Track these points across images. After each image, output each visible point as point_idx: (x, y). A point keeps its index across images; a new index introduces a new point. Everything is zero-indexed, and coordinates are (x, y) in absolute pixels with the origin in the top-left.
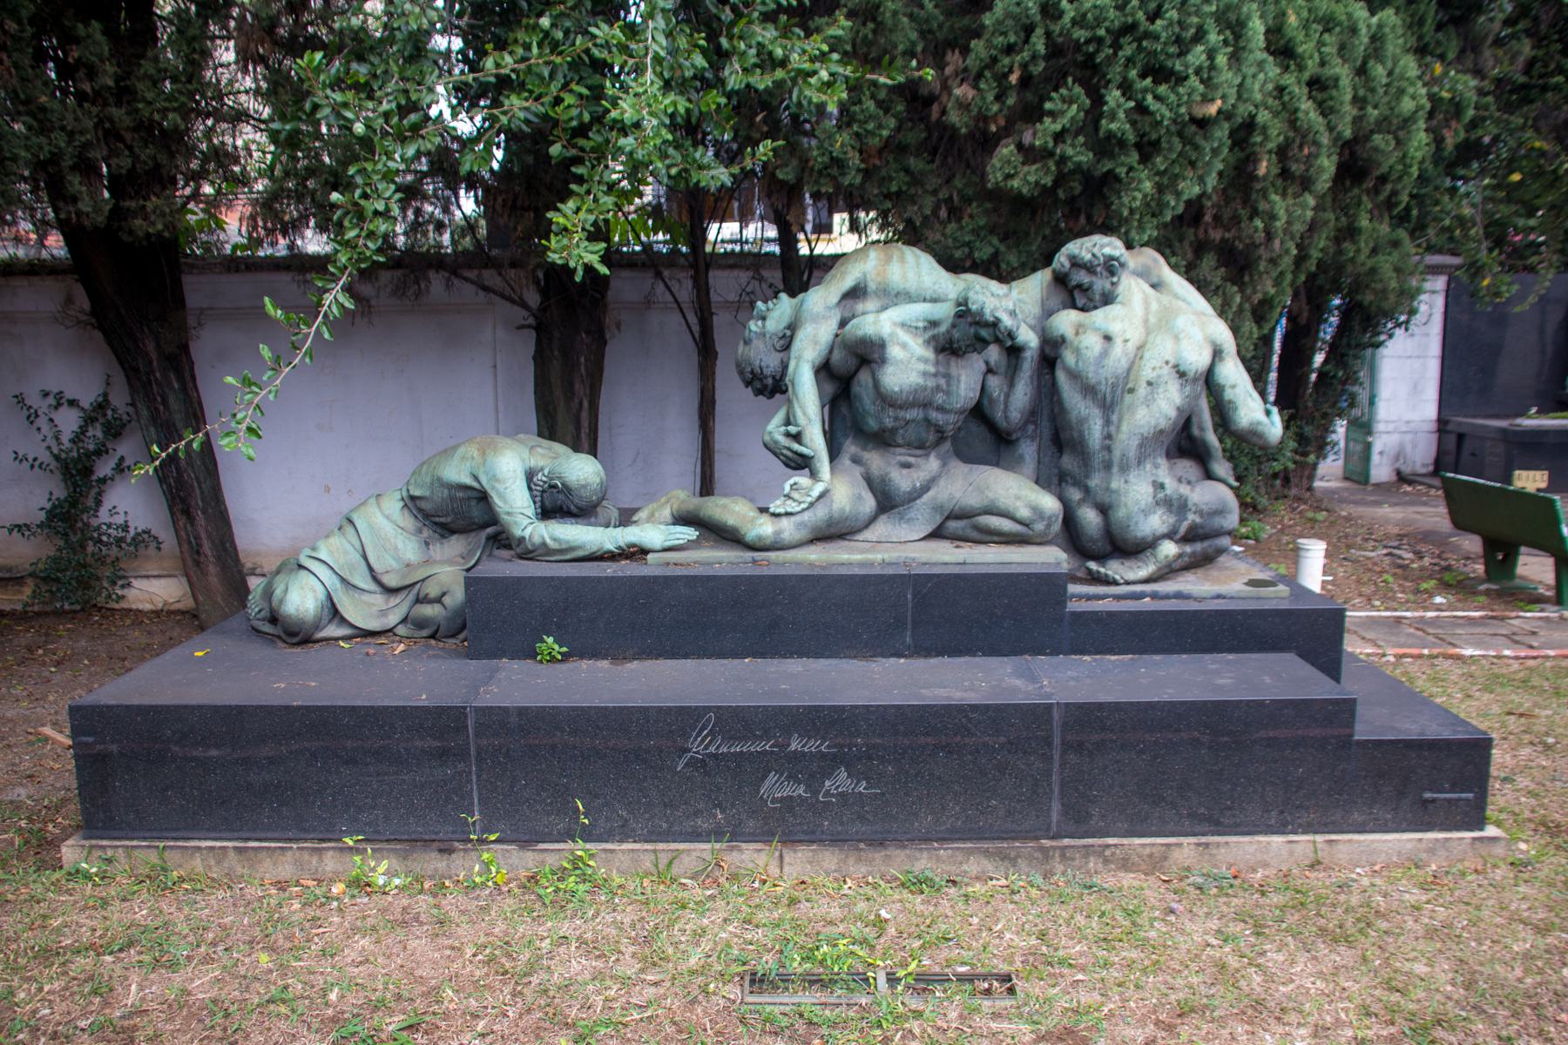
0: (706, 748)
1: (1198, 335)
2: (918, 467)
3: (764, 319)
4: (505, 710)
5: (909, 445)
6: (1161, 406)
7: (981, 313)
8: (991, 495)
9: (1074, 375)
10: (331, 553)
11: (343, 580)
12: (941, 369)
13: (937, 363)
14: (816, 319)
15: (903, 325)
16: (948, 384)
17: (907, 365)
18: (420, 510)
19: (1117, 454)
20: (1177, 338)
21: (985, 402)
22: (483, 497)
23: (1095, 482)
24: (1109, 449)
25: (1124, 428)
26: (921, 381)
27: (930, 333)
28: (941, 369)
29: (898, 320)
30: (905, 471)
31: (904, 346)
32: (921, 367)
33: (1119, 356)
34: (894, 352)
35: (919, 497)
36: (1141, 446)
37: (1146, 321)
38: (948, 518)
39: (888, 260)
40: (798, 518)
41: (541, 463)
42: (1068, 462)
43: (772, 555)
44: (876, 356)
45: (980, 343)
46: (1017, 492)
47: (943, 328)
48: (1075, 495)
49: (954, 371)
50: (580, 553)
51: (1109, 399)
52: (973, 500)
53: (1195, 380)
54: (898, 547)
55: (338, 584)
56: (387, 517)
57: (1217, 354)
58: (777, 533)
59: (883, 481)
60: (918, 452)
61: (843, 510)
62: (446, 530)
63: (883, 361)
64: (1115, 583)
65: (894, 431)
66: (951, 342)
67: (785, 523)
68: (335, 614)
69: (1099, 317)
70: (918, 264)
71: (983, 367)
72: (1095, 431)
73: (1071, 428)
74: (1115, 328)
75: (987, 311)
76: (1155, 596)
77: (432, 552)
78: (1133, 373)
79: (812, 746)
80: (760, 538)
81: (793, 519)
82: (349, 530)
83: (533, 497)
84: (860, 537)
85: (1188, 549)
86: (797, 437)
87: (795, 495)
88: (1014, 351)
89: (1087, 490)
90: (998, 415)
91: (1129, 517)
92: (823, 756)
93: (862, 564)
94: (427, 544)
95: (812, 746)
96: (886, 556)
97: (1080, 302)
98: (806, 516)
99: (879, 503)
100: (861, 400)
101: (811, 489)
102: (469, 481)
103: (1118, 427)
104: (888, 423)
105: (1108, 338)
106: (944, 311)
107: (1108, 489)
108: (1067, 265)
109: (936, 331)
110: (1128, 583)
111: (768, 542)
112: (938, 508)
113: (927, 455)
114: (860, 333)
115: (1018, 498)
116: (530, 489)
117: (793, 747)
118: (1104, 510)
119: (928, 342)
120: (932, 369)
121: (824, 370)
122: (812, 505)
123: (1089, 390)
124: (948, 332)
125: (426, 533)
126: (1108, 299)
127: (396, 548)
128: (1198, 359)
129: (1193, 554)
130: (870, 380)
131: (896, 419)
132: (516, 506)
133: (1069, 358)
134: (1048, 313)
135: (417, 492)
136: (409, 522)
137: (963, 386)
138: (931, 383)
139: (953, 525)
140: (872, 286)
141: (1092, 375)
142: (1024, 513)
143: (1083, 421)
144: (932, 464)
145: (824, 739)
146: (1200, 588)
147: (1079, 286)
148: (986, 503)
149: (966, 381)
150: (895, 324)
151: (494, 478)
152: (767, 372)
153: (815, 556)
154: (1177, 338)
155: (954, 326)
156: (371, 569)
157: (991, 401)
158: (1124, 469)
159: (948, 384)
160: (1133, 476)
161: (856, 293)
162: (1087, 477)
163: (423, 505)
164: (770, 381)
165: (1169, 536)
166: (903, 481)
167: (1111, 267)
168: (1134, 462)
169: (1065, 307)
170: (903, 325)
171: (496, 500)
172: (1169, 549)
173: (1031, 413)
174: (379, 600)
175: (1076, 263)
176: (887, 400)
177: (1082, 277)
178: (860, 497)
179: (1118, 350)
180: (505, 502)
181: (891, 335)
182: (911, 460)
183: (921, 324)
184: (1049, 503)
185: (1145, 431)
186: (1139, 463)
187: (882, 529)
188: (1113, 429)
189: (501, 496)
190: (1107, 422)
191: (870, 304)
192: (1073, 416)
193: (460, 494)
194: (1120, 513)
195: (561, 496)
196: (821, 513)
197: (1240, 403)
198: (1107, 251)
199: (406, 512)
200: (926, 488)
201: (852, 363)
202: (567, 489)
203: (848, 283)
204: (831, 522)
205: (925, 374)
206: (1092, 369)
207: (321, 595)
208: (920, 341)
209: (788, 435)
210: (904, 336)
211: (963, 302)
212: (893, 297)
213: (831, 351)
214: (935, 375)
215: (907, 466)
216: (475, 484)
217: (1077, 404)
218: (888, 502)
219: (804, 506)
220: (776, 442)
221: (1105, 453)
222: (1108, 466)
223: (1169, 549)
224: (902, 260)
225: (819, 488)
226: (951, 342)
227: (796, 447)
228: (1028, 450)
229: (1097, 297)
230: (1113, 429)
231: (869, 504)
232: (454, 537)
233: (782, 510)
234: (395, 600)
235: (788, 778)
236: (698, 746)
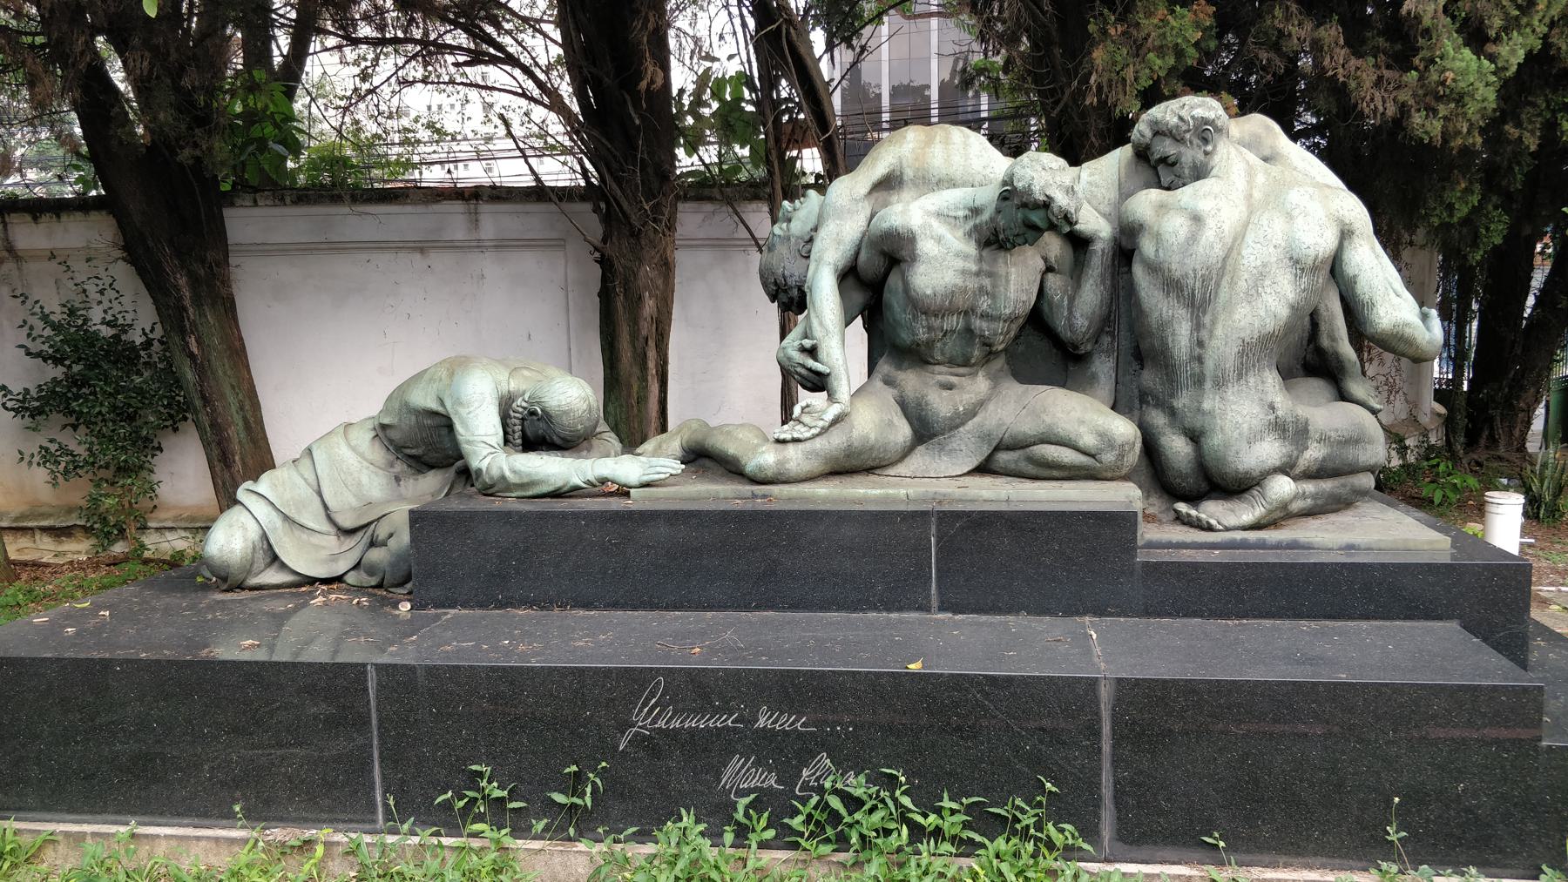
0: (654, 721)
1: (1317, 210)
2: (962, 388)
3: (789, 220)
4: (411, 669)
5: (952, 362)
6: (1265, 304)
7: (1028, 191)
8: (1048, 420)
9: (1154, 268)
10: (274, 486)
11: (286, 518)
13: (980, 259)
14: (841, 214)
15: (939, 215)
16: (994, 286)
17: (942, 263)
18: (391, 441)
19: (1209, 364)
20: (1290, 217)
21: (1046, 308)
23: (1182, 401)
25: (1219, 331)
26: (959, 281)
27: (971, 224)
28: (985, 267)
29: (932, 208)
30: (945, 393)
32: (960, 264)
33: (1211, 242)
34: (926, 247)
35: (963, 424)
36: (1241, 354)
37: (1249, 197)
38: (997, 449)
39: (929, 142)
40: (807, 446)
43: (775, 490)
44: (904, 253)
45: (1031, 232)
46: (1085, 416)
47: (985, 216)
48: (1158, 419)
49: (1001, 269)
50: (545, 489)
51: (1198, 296)
52: (1027, 427)
53: (1315, 269)
54: (938, 480)
55: (277, 521)
56: (354, 449)
57: (1345, 234)
58: (780, 463)
60: (962, 370)
61: (866, 438)
63: (914, 258)
64: (1210, 528)
65: (930, 344)
66: (996, 233)
67: (792, 451)
68: (274, 559)
69: (1187, 195)
70: (966, 145)
71: (1041, 265)
72: (1181, 336)
73: (1151, 334)
74: (1204, 206)
75: (1036, 188)
76: (1261, 545)
77: (402, 489)
78: (1230, 261)
79: (785, 722)
80: (760, 468)
81: (801, 446)
82: (306, 462)
84: (891, 471)
85: (1309, 487)
86: (812, 352)
87: (806, 419)
88: (1079, 243)
89: (1172, 413)
90: (1060, 324)
91: (1227, 446)
92: (800, 735)
93: (877, 500)
94: (397, 479)
95: (785, 722)
96: (911, 491)
97: (1166, 179)
98: (818, 444)
99: (915, 431)
100: (890, 307)
101: (824, 411)
104: (922, 335)
105: (1197, 219)
106: (987, 196)
108: (1148, 133)
110: (1227, 529)
111: (770, 473)
112: (985, 437)
113: (974, 374)
114: (885, 225)
117: (761, 723)
118: (1195, 437)
120: (974, 268)
121: (849, 275)
122: (824, 431)
123: (1173, 286)
125: (400, 467)
126: (1200, 173)
127: (359, 484)
128: (1321, 242)
129: (1314, 496)
130: (900, 284)
131: (930, 328)
133: (1147, 247)
134: (1125, 194)
135: (386, 421)
136: (378, 454)
137: (1012, 288)
138: (972, 284)
139: (1004, 457)
140: (909, 173)
141: (1176, 270)
142: (1088, 440)
143: (1164, 325)
144: (979, 385)
145: (800, 715)
146: (1328, 537)
147: (1163, 160)
148: (1042, 429)
149: (1019, 280)
150: (928, 213)
151: (458, 402)
153: (826, 493)
154: (1290, 217)
155: (998, 211)
156: (326, 507)
157: (1050, 304)
158: (1220, 383)
159: (994, 286)
160: (1231, 393)
161: (888, 184)
162: (1172, 395)
165: (1285, 469)
166: (941, 404)
167: (1205, 132)
168: (1233, 375)
169: (1148, 186)
170: (939, 215)
171: (458, 427)
172: (1282, 487)
173: (1097, 320)
174: (331, 542)
175: (1159, 131)
176: (919, 307)
177: (1167, 148)
178: (890, 424)
179: (1209, 235)
180: (466, 427)
181: (923, 226)
182: (954, 379)
183: (961, 213)
184: (1123, 429)
185: (1246, 335)
186: (1240, 376)
187: (919, 461)
188: (1204, 334)
189: (463, 423)
190: (1198, 326)
191: (906, 194)
192: (1153, 319)
194: (1214, 441)
195: (541, 425)
196: (835, 442)
197: (1378, 299)
198: (1199, 112)
200: (971, 413)
202: (547, 417)
204: (850, 452)
205: (964, 272)
206: (1176, 258)
207: (253, 533)
208: (960, 233)
209: (803, 350)
210: (940, 228)
211: (1008, 181)
212: (930, 182)
214: (978, 274)
216: (440, 409)
217: (1156, 302)
218: (925, 431)
219: (814, 431)
220: (789, 359)
221: (1196, 365)
222: (1199, 381)
223: (1282, 487)
224: (947, 141)
225: (834, 410)
226: (996, 233)
227: (811, 363)
228: (1103, 367)
229: (1187, 171)
230: (1204, 334)
231: (903, 431)
233: (788, 436)
234: (350, 542)
235: (757, 764)
236: (643, 721)
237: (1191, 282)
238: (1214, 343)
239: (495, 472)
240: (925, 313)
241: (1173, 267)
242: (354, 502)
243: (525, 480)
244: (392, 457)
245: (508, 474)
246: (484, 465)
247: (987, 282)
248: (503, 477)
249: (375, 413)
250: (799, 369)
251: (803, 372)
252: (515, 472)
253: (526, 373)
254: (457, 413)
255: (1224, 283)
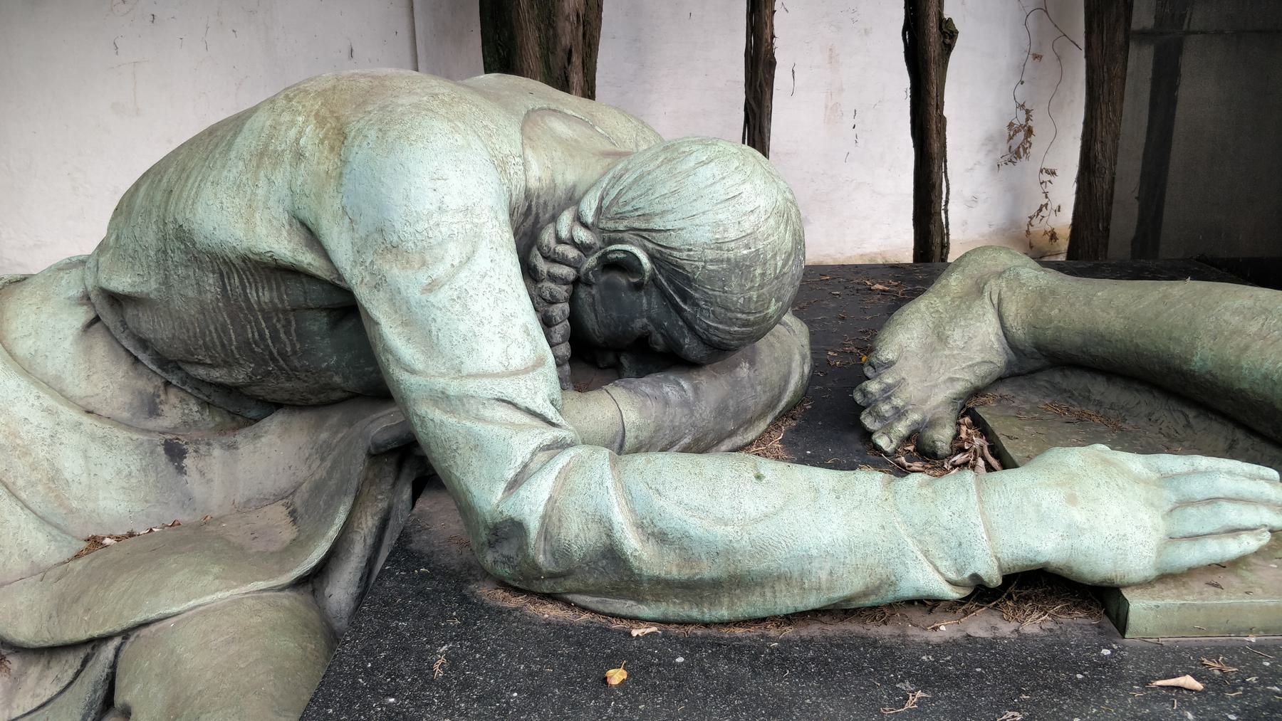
22: (344, 309)
41: (569, 175)
62: (240, 405)
77: (192, 479)
83: (542, 305)
94: (175, 452)
102: (283, 245)
116: (529, 273)
125: (177, 411)
127: (54, 478)
132: (474, 343)
135: (122, 283)
136: (106, 378)
151: (382, 241)
163: (145, 323)
171: (394, 337)
180: (430, 344)
193: (263, 296)
195: (648, 303)
199: (100, 347)
202: (673, 278)
216: (307, 259)
232: (273, 426)
239: (578, 534)
242: (44, 547)
243: (707, 571)
244: (148, 385)
245: (632, 543)
246: (531, 505)
248: (612, 555)
249: (86, 245)
252: (661, 538)
253: (559, 127)
254: (379, 282)
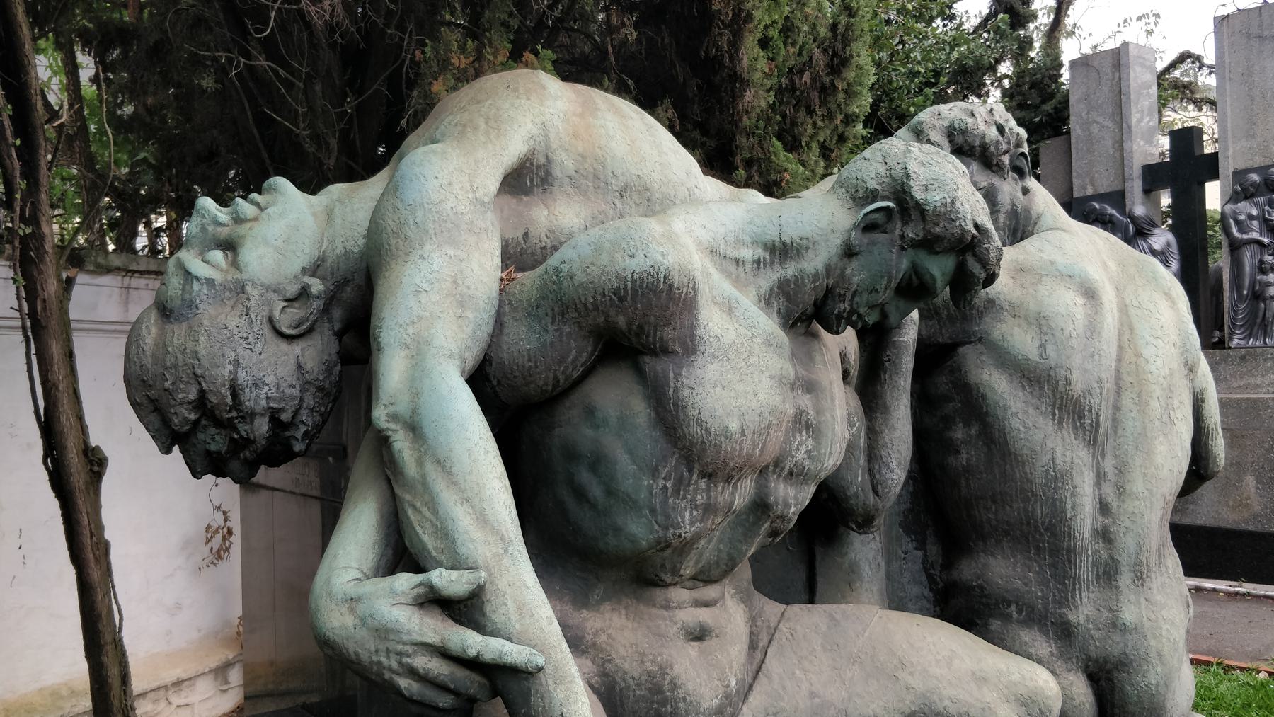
3: (230, 246)
8: (917, 683)
12: (802, 372)
15: (713, 252)
16: (818, 412)
24: (1105, 536)
25: (1137, 485)
27: (770, 278)
28: (802, 372)
29: (705, 236)
30: (693, 649)
31: (729, 308)
34: (713, 322)
42: (1001, 570)
44: (669, 334)
47: (814, 263)
59: (657, 690)
63: (690, 347)
73: (1028, 495)
103: (1120, 488)
107: (1116, 625)
109: (790, 270)
114: (637, 265)
115: (982, 680)
119: (766, 301)
121: (481, 380)
124: (828, 269)
130: (640, 410)
140: (565, 163)
143: (1058, 478)
152: (250, 399)
155: (849, 252)
159: (818, 412)
162: (1065, 600)
164: (262, 427)
183: (748, 254)
188: (1109, 491)
190: (1100, 477)
201: (578, 351)
203: (513, 148)
206: (1076, 360)
209: (435, 601)
213: (499, 324)
215: (699, 635)
220: (384, 632)
221: (1099, 546)
222: (1107, 574)
227: (471, 642)
237: (1095, 401)
238: (1130, 505)
240: (709, 476)
241: (1075, 375)
247: (806, 401)
250: (422, 662)
251: (437, 667)
255: (1127, 401)
